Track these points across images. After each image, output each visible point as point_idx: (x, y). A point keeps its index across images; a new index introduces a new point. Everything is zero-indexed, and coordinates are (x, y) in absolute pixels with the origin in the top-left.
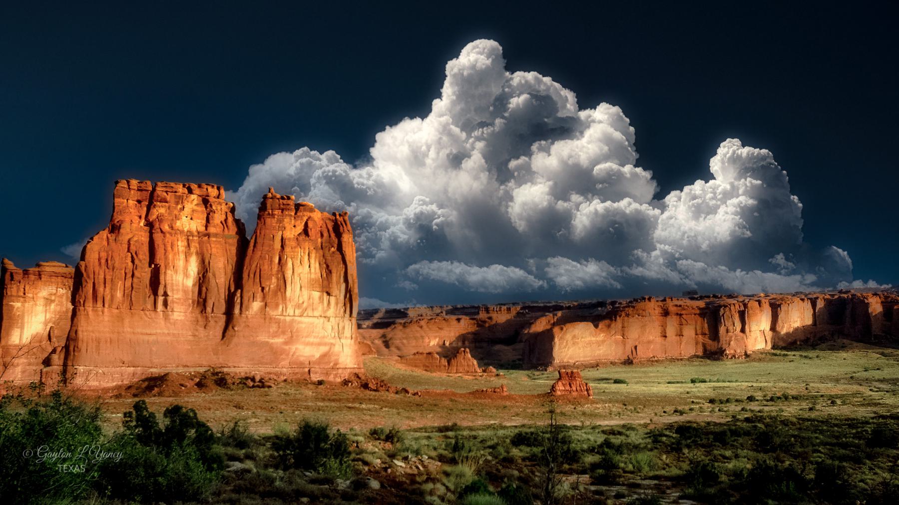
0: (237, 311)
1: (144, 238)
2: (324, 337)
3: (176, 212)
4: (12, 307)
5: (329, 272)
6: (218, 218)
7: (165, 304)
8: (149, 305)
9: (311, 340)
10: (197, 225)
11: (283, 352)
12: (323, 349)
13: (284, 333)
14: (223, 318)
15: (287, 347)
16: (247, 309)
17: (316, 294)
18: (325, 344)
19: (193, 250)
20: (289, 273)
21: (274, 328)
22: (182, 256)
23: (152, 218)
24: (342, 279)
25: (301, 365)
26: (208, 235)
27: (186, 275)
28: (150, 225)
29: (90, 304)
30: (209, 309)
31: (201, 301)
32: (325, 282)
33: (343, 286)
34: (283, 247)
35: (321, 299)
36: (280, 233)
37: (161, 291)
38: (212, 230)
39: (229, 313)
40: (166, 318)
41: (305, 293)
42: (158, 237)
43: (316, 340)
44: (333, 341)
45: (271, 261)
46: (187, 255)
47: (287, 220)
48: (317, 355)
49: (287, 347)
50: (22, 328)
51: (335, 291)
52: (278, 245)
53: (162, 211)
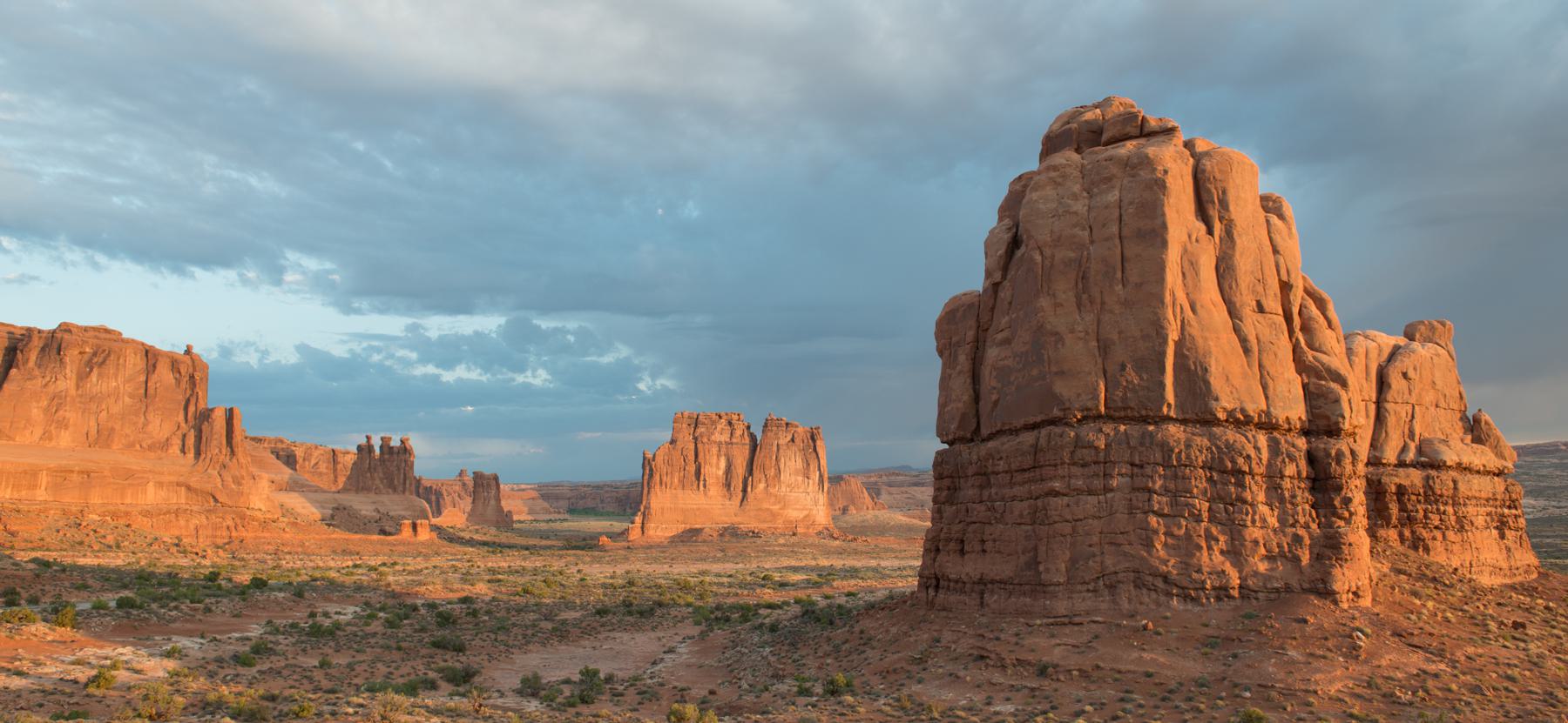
0: (749, 489)
5: (808, 465)
6: (738, 433)
7: (705, 486)
8: (695, 487)
10: (725, 438)
12: (806, 513)
17: (800, 478)
20: (782, 466)
21: (773, 500)
27: (718, 468)
28: (695, 439)
29: (658, 487)
31: (728, 485)
34: (778, 450)
38: (734, 440)
39: (745, 491)
40: (705, 494)
42: (699, 446)
48: (801, 516)
51: (812, 476)
52: (775, 448)
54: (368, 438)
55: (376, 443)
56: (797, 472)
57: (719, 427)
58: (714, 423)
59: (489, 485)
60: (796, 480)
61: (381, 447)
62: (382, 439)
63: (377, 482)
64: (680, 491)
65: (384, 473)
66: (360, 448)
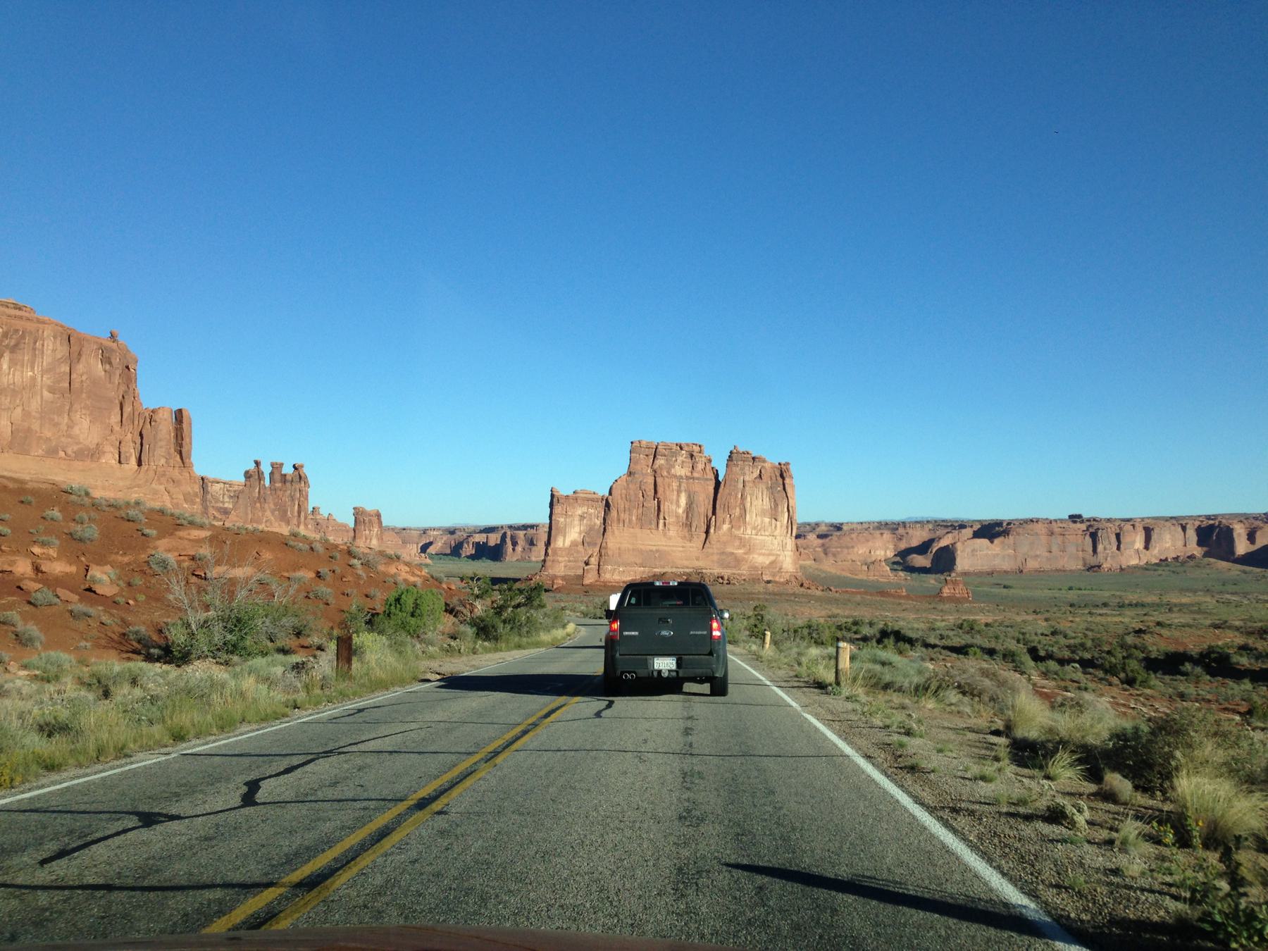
0: (712, 530)
1: (651, 480)
2: (771, 550)
3: (671, 463)
4: (558, 521)
6: (700, 466)
8: (653, 526)
9: (763, 551)
11: (744, 559)
12: (772, 558)
13: (744, 546)
14: (705, 535)
15: (746, 556)
16: (720, 528)
17: (767, 520)
18: (773, 555)
19: (682, 488)
20: (748, 505)
22: (675, 493)
23: (656, 466)
24: (786, 509)
25: (755, 568)
26: (693, 478)
27: (678, 506)
30: (693, 529)
31: (688, 525)
32: (773, 512)
33: (786, 514)
35: (770, 524)
36: (742, 478)
37: (661, 517)
40: (665, 535)
41: (759, 519)
43: (767, 552)
44: (778, 553)
45: (736, 496)
46: (679, 492)
47: (747, 468)
48: (767, 562)
49: (746, 556)
50: (565, 537)
53: (662, 462)
54: (257, 463)
55: (266, 469)
56: (763, 513)
57: (680, 459)
58: (674, 454)
59: (370, 521)
60: (762, 522)
61: (272, 474)
62: (272, 465)
63: (268, 513)
64: (638, 530)
65: (275, 504)
66: (248, 475)
